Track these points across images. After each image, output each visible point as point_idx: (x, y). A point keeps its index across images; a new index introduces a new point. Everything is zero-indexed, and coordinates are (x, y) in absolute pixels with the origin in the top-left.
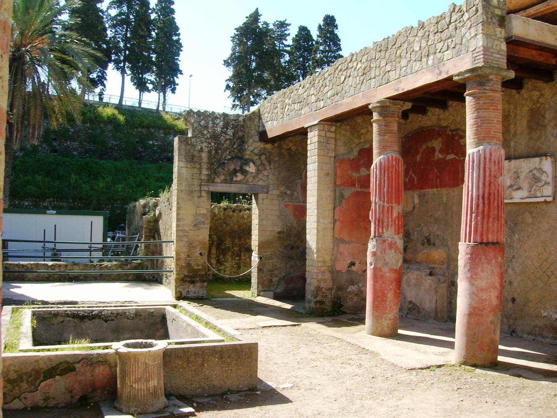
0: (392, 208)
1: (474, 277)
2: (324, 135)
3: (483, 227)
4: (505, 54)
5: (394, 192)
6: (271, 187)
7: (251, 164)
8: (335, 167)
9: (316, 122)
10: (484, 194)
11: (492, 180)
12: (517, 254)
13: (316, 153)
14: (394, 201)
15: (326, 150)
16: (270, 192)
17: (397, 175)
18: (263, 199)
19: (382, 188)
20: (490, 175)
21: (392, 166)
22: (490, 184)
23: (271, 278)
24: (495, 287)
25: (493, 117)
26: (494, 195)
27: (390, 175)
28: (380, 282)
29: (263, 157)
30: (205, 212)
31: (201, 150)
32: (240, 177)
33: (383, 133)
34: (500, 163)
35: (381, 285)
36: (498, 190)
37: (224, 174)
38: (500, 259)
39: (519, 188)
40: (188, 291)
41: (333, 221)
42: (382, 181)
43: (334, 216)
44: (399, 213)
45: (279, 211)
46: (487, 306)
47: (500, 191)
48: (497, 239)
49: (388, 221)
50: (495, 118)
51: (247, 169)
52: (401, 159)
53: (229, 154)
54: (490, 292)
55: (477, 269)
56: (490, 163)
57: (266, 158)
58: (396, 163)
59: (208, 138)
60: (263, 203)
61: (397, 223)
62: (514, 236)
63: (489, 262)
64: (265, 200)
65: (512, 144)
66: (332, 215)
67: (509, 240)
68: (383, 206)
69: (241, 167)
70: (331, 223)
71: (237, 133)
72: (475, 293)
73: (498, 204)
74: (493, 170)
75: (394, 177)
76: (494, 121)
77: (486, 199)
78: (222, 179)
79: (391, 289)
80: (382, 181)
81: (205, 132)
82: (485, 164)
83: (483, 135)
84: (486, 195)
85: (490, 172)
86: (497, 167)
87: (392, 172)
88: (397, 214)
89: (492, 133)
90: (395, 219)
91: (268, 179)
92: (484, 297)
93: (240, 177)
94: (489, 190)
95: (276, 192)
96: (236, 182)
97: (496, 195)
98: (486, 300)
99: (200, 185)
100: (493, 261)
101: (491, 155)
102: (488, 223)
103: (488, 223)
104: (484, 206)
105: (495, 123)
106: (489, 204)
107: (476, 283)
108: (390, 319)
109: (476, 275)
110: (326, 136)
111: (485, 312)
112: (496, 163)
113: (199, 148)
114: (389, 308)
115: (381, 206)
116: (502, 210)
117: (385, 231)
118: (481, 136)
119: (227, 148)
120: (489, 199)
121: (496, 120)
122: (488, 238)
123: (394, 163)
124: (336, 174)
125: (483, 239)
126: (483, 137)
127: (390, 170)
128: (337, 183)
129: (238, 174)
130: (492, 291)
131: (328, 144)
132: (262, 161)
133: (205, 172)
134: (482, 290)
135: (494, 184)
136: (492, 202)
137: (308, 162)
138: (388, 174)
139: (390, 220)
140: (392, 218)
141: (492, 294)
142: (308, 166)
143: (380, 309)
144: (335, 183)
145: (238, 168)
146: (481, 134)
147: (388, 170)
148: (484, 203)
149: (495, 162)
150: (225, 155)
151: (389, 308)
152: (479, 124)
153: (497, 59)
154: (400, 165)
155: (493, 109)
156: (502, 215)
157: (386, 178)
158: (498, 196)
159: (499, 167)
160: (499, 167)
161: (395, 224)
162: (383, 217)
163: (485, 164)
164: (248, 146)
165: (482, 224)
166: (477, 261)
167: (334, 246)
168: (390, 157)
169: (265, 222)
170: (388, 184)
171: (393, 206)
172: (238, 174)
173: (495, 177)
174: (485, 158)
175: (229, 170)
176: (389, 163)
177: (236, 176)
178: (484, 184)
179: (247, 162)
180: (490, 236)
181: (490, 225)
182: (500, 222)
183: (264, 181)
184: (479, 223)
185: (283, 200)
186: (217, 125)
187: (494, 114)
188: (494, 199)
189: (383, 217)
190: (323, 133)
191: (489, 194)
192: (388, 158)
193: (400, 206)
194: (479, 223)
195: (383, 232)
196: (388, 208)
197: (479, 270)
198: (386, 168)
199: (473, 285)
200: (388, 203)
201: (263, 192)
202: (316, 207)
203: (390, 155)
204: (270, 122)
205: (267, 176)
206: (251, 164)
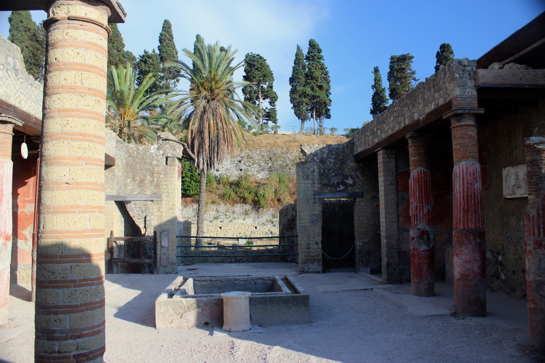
0: (423, 207)
1: (461, 253)
2: (387, 157)
3: (464, 219)
4: (477, 97)
5: (424, 195)
6: (365, 193)
7: (350, 179)
8: (397, 179)
9: (380, 148)
10: (464, 196)
11: (469, 186)
12: (522, 235)
13: (382, 170)
14: (424, 202)
15: (389, 167)
16: (364, 197)
17: (425, 184)
18: (360, 202)
19: (415, 193)
20: (467, 183)
21: (421, 178)
22: (468, 189)
23: (368, 258)
24: (476, 260)
25: (467, 143)
26: (471, 196)
27: (420, 184)
28: (418, 258)
29: (358, 172)
30: (318, 213)
31: (314, 171)
32: (342, 188)
33: (414, 155)
34: (475, 174)
35: (418, 260)
36: (475, 193)
37: (330, 186)
38: (479, 241)
39: (519, 187)
40: (309, 268)
41: (397, 216)
42: (415, 189)
43: (398, 213)
44: (428, 210)
45: (371, 210)
46: (471, 274)
47: (476, 193)
48: (476, 226)
49: (420, 216)
50: (470, 143)
51: (347, 181)
52: (428, 171)
53: (333, 172)
54: (473, 264)
55: (462, 248)
56: (467, 175)
57: (360, 173)
58: (424, 175)
59: (317, 162)
60: (359, 205)
61: (427, 217)
62: (521, 223)
63: (470, 243)
64: (361, 203)
65: (514, 154)
66: (396, 212)
67: (517, 225)
68: (417, 206)
69: (342, 180)
70: (395, 217)
71: (338, 157)
72: (462, 264)
73: (475, 202)
74: (469, 179)
75: (423, 185)
76: (469, 145)
77: (465, 200)
78: (329, 189)
79: (426, 263)
80: (415, 189)
81: (316, 158)
82: (463, 176)
83: (461, 156)
84: (465, 197)
85: (467, 181)
86: (472, 177)
87: (421, 182)
88: (427, 211)
89: (468, 153)
90: (426, 214)
91: (363, 187)
92: (468, 267)
93: (342, 188)
94: (468, 193)
95: (369, 196)
96: (339, 191)
97: (473, 196)
98: (469, 269)
99: (314, 195)
100: (473, 242)
101: (467, 169)
102: (468, 216)
103: (468, 216)
104: (464, 205)
105: (470, 147)
106: (468, 203)
107: (462, 257)
108: (425, 284)
109: (462, 252)
110: (388, 157)
111: (470, 278)
112: (472, 174)
113: (312, 169)
114: (424, 277)
115: (416, 205)
116: (480, 206)
117: (419, 223)
118: (460, 156)
119: (332, 168)
120: (467, 199)
121: (470, 144)
122: (468, 226)
123: (423, 175)
124: (397, 183)
125: (465, 227)
126: (462, 157)
127: (420, 180)
128: (399, 189)
129: (340, 186)
130: (474, 263)
131: (390, 162)
132: (357, 175)
133: (317, 185)
134: (466, 262)
135: (470, 189)
136: (469, 202)
137: (379, 176)
138: (419, 183)
139: (422, 215)
140: (423, 213)
141: (474, 265)
142: (379, 178)
143: (418, 277)
144: (397, 189)
145: (340, 181)
146: (460, 155)
147: (418, 180)
148: (464, 202)
149: (471, 174)
150: (330, 172)
151: (424, 277)
152: (459, 149)
153: (468, 102)
154: (428, 176)
155: (467, 137)
156: (480, 210)
157: (417, 186)
158: (475, 197)
159: (474, 177)
160: (474, 177)
161: (426, 217)
162: (417, 214)
163: (463, 176)
164: (347, 165)
165: (464, 217)
166: (461, 242)
167: (399, 233)
168: (420, 172)
169: (362, 218)
170: (419, 190)
171: (424, 205)
172: (340, 186)
173: (471, 184)
174: (463, 172)
175: (333, 183)
176: (418, 176)
177: (339, 187)
178: (463, 189)
179: (347, 177)
180: (470, 224)
181: (469, 217)
182: (477, 215)
183: (359, 189)
184: (462, 216)
185: (374, 202)
186: (323, 153)
187: (468, 140)
188: (472, 199)
189: (417, 214)
190: (386, 156)
191: (468, 196)
192: (418, 172)
193: (429, 206)
194: (462, 216)
195: (417, 224)
196: (420, 207)
197: (464, 248)
198: (417, 179)
199: (460, 259)
200: (419, 203)
201: (360, 197)
202: (384, 207)
203: (419, 170)
204: (359, 148)
205: (362, 185)
206: (350, 179)
